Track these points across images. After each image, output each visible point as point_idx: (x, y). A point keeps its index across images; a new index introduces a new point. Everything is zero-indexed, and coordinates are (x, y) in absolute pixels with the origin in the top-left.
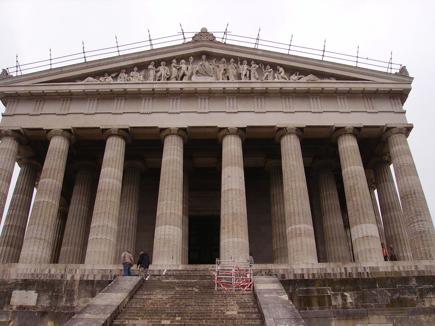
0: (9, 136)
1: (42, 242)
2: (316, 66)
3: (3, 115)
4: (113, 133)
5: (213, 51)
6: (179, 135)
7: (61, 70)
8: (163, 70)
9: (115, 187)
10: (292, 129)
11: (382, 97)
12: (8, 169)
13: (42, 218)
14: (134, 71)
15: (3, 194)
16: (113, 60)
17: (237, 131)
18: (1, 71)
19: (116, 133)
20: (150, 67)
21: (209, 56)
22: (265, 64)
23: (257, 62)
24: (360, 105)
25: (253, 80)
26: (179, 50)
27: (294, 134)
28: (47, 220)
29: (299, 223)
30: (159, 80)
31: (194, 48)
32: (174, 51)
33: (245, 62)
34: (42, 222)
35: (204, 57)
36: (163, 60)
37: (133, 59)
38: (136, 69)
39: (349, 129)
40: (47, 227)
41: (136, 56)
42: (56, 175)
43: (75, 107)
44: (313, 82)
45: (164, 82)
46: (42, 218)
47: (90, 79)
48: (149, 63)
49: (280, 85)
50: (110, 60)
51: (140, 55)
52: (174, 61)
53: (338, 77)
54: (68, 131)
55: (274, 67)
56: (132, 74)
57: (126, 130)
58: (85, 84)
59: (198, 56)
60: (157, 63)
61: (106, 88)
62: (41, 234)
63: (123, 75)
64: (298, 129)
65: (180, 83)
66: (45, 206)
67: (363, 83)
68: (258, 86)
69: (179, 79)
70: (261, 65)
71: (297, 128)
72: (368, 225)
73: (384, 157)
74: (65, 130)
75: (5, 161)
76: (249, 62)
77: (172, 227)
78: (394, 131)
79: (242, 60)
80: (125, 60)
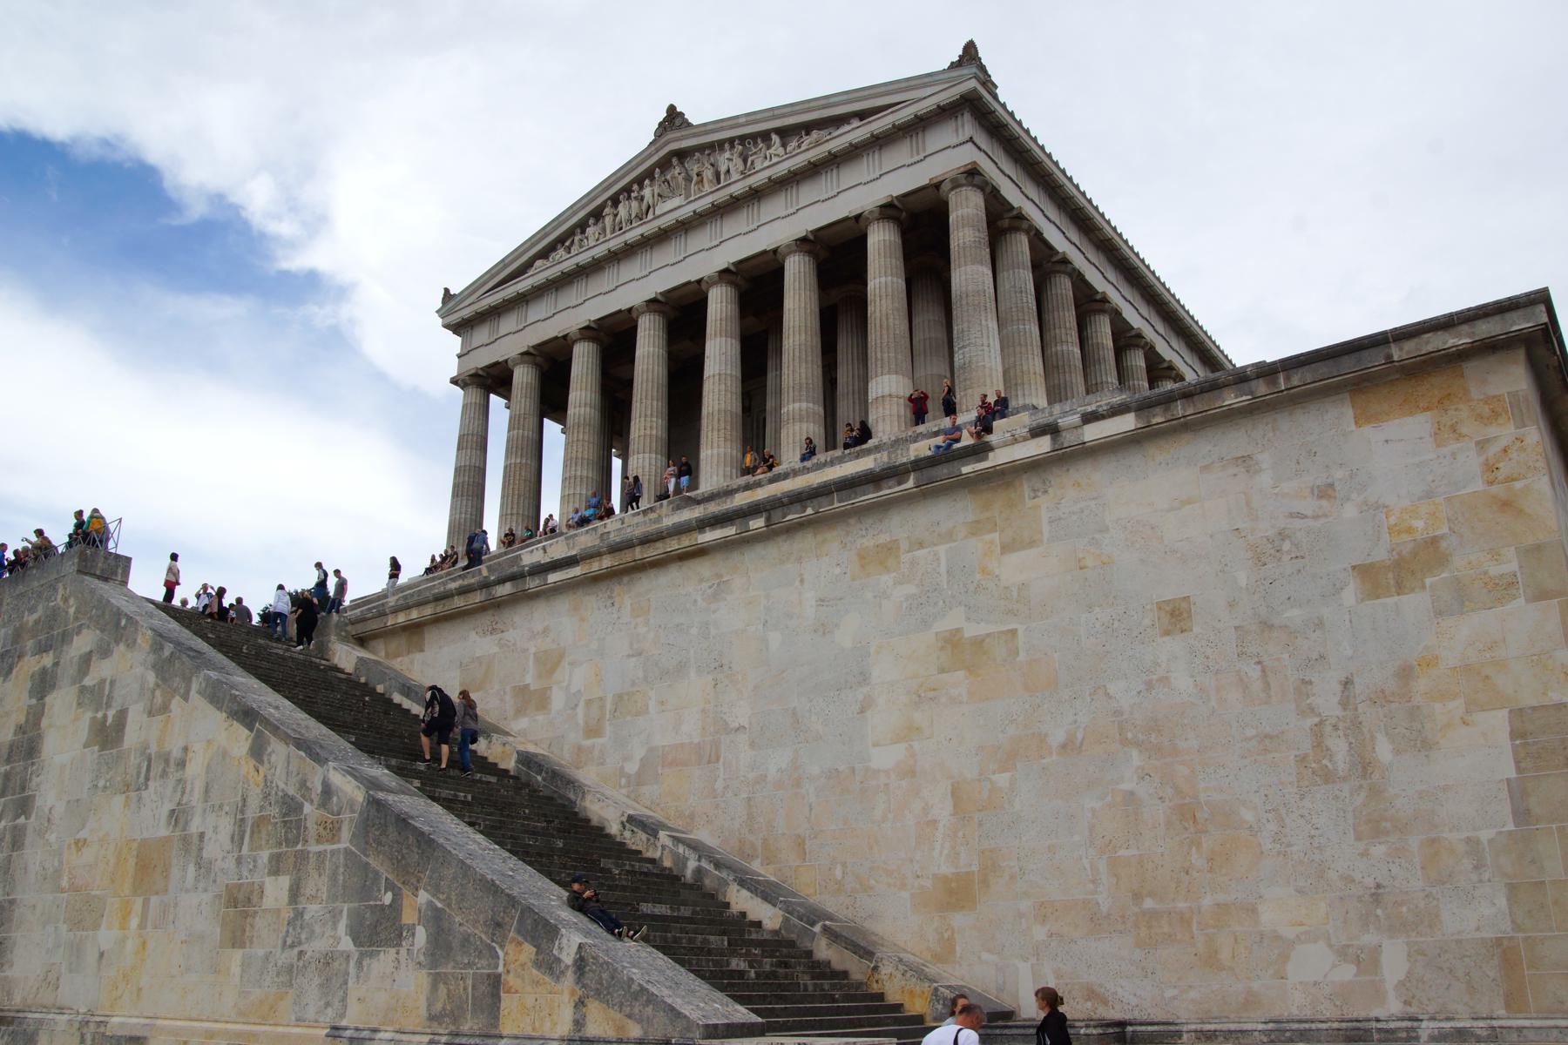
0: (470, 385)
1: (515, 518)
2: (824, 108)
3: (459, 356)
4: (574, 338)
5: (682, 146)
6: (651, 312)
7: (504, 263)
8: (622, 210)
9: (582, 419)
10: (788, 246)
11: (937, 122)
12: (475, 432)
13: (511, 487)
14: (589, 226)
15: (475, 467)
16: (561, 219)
17: (719, 276)
18: (443, 292)
19: (579, 336)
21: (682, 155)
22: (754, 137)
24: (900, 154)
26: (638, 165)
27: (795, 252)
28: (516, 487)
29: (800, 401)
30: (621, 229)
31: (657, 152)
32: (633, 169)
33: (727, 146)
34: (511, 492)
35: (675, 161)
36: (618, 194)
37: (583, 207)
38: (591, 221)
39: (871, 212)
40: (519, 496)
41: (586, 200)
42: (522, 423)
44: (818, 144)
45: (628, 228)
46: (511, 487)
47: (539, 263)
48: (602, 206)
49: (767, 173)
50: (551, 227)
51: (590, 196)
52: (635, 187)
53: (862, 115)
54: (526, 353)
55: (765, 136)
57: (587, 328)
58: (532, 275)
60: (615, 201)
61: (568, 265)
62: (512, 508)
64: (798, 243)
65: (620, 235)
66: (512, 469)
67: (892, 112)
69: (644, 216)
70: (749, 144)
71: (796, 240)
72: (886, 378)
73: (999, 223)
74: (523, 354)
75: (469, 422)
77: (647, 455)
78: (945, 187)
80: (575, 213)
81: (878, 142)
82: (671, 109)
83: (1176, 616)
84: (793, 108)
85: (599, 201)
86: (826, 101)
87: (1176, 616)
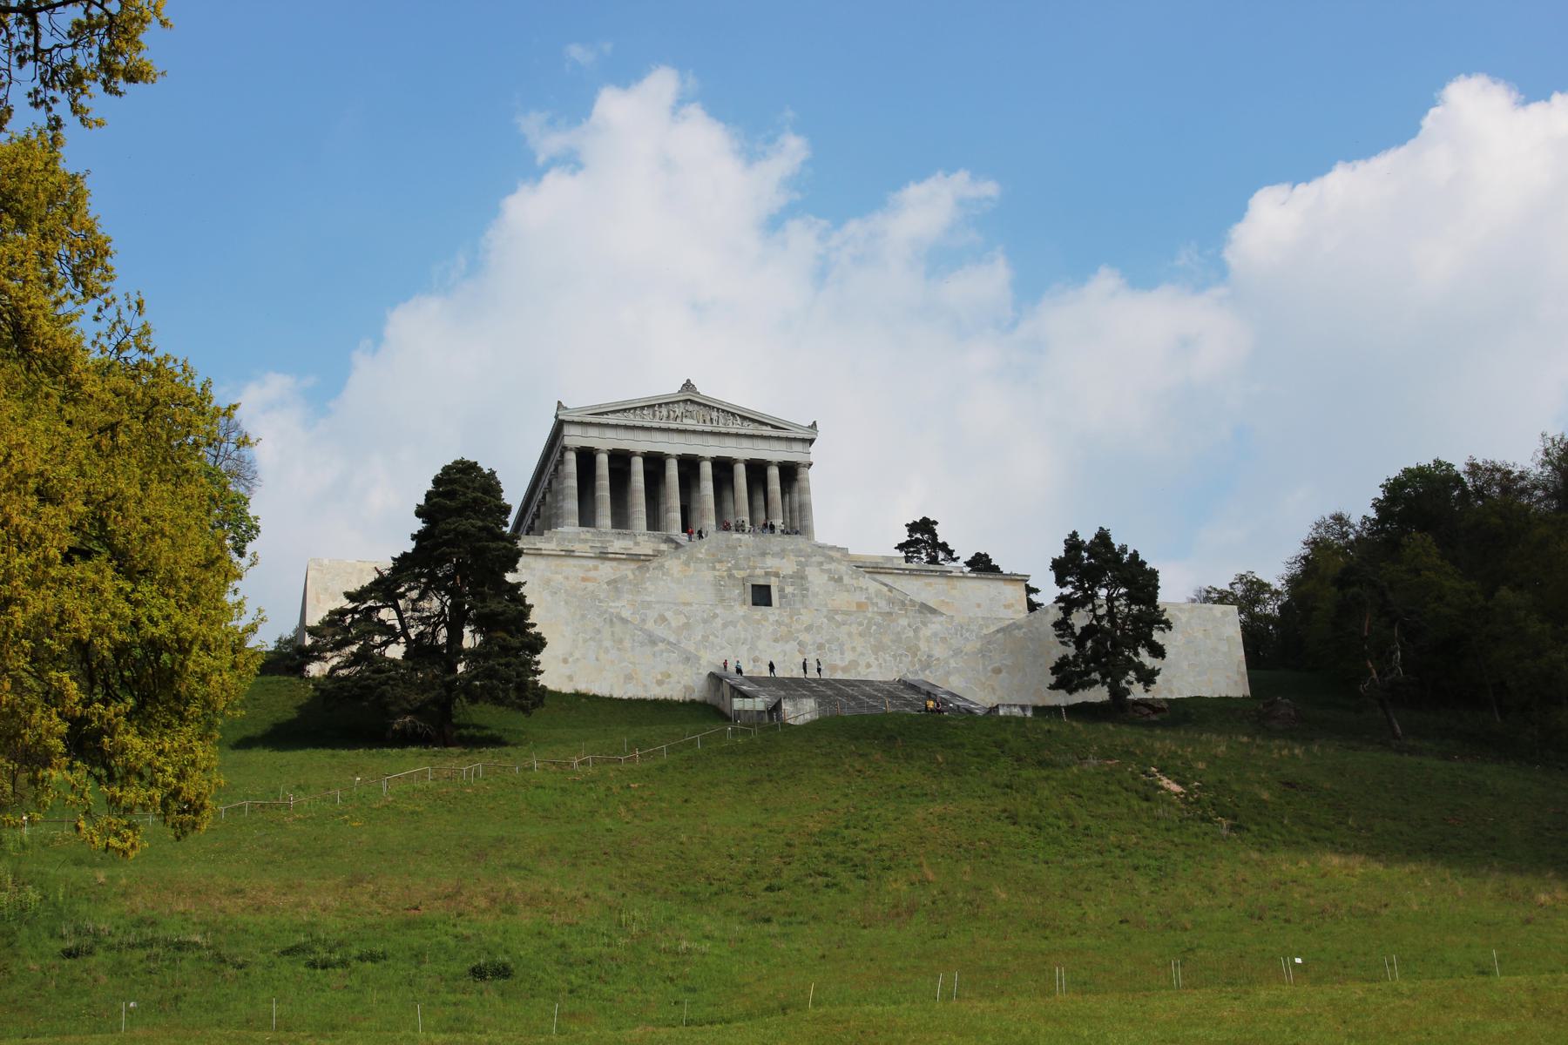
8: (664, 412)
20: (656, 408)
21: (692, 402)
23: (723, 411)
24: (782, 446)
25: (720, 425)
43: (610, 433)
53: (774, 427)
56: (645, 412)
59: (686, 401)
60: (660, 405)
63: (638, 412)
68: (723, 430)
76: (718, 409)
79: (714, 407)
81: (779, 438)
82: (688, 381)
83: (979, 606)
84: (748, 411)
85: (653, 403)
86: (762, 415)
87: (979, 606)
